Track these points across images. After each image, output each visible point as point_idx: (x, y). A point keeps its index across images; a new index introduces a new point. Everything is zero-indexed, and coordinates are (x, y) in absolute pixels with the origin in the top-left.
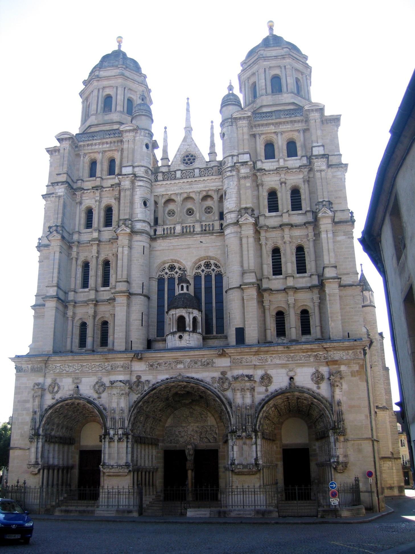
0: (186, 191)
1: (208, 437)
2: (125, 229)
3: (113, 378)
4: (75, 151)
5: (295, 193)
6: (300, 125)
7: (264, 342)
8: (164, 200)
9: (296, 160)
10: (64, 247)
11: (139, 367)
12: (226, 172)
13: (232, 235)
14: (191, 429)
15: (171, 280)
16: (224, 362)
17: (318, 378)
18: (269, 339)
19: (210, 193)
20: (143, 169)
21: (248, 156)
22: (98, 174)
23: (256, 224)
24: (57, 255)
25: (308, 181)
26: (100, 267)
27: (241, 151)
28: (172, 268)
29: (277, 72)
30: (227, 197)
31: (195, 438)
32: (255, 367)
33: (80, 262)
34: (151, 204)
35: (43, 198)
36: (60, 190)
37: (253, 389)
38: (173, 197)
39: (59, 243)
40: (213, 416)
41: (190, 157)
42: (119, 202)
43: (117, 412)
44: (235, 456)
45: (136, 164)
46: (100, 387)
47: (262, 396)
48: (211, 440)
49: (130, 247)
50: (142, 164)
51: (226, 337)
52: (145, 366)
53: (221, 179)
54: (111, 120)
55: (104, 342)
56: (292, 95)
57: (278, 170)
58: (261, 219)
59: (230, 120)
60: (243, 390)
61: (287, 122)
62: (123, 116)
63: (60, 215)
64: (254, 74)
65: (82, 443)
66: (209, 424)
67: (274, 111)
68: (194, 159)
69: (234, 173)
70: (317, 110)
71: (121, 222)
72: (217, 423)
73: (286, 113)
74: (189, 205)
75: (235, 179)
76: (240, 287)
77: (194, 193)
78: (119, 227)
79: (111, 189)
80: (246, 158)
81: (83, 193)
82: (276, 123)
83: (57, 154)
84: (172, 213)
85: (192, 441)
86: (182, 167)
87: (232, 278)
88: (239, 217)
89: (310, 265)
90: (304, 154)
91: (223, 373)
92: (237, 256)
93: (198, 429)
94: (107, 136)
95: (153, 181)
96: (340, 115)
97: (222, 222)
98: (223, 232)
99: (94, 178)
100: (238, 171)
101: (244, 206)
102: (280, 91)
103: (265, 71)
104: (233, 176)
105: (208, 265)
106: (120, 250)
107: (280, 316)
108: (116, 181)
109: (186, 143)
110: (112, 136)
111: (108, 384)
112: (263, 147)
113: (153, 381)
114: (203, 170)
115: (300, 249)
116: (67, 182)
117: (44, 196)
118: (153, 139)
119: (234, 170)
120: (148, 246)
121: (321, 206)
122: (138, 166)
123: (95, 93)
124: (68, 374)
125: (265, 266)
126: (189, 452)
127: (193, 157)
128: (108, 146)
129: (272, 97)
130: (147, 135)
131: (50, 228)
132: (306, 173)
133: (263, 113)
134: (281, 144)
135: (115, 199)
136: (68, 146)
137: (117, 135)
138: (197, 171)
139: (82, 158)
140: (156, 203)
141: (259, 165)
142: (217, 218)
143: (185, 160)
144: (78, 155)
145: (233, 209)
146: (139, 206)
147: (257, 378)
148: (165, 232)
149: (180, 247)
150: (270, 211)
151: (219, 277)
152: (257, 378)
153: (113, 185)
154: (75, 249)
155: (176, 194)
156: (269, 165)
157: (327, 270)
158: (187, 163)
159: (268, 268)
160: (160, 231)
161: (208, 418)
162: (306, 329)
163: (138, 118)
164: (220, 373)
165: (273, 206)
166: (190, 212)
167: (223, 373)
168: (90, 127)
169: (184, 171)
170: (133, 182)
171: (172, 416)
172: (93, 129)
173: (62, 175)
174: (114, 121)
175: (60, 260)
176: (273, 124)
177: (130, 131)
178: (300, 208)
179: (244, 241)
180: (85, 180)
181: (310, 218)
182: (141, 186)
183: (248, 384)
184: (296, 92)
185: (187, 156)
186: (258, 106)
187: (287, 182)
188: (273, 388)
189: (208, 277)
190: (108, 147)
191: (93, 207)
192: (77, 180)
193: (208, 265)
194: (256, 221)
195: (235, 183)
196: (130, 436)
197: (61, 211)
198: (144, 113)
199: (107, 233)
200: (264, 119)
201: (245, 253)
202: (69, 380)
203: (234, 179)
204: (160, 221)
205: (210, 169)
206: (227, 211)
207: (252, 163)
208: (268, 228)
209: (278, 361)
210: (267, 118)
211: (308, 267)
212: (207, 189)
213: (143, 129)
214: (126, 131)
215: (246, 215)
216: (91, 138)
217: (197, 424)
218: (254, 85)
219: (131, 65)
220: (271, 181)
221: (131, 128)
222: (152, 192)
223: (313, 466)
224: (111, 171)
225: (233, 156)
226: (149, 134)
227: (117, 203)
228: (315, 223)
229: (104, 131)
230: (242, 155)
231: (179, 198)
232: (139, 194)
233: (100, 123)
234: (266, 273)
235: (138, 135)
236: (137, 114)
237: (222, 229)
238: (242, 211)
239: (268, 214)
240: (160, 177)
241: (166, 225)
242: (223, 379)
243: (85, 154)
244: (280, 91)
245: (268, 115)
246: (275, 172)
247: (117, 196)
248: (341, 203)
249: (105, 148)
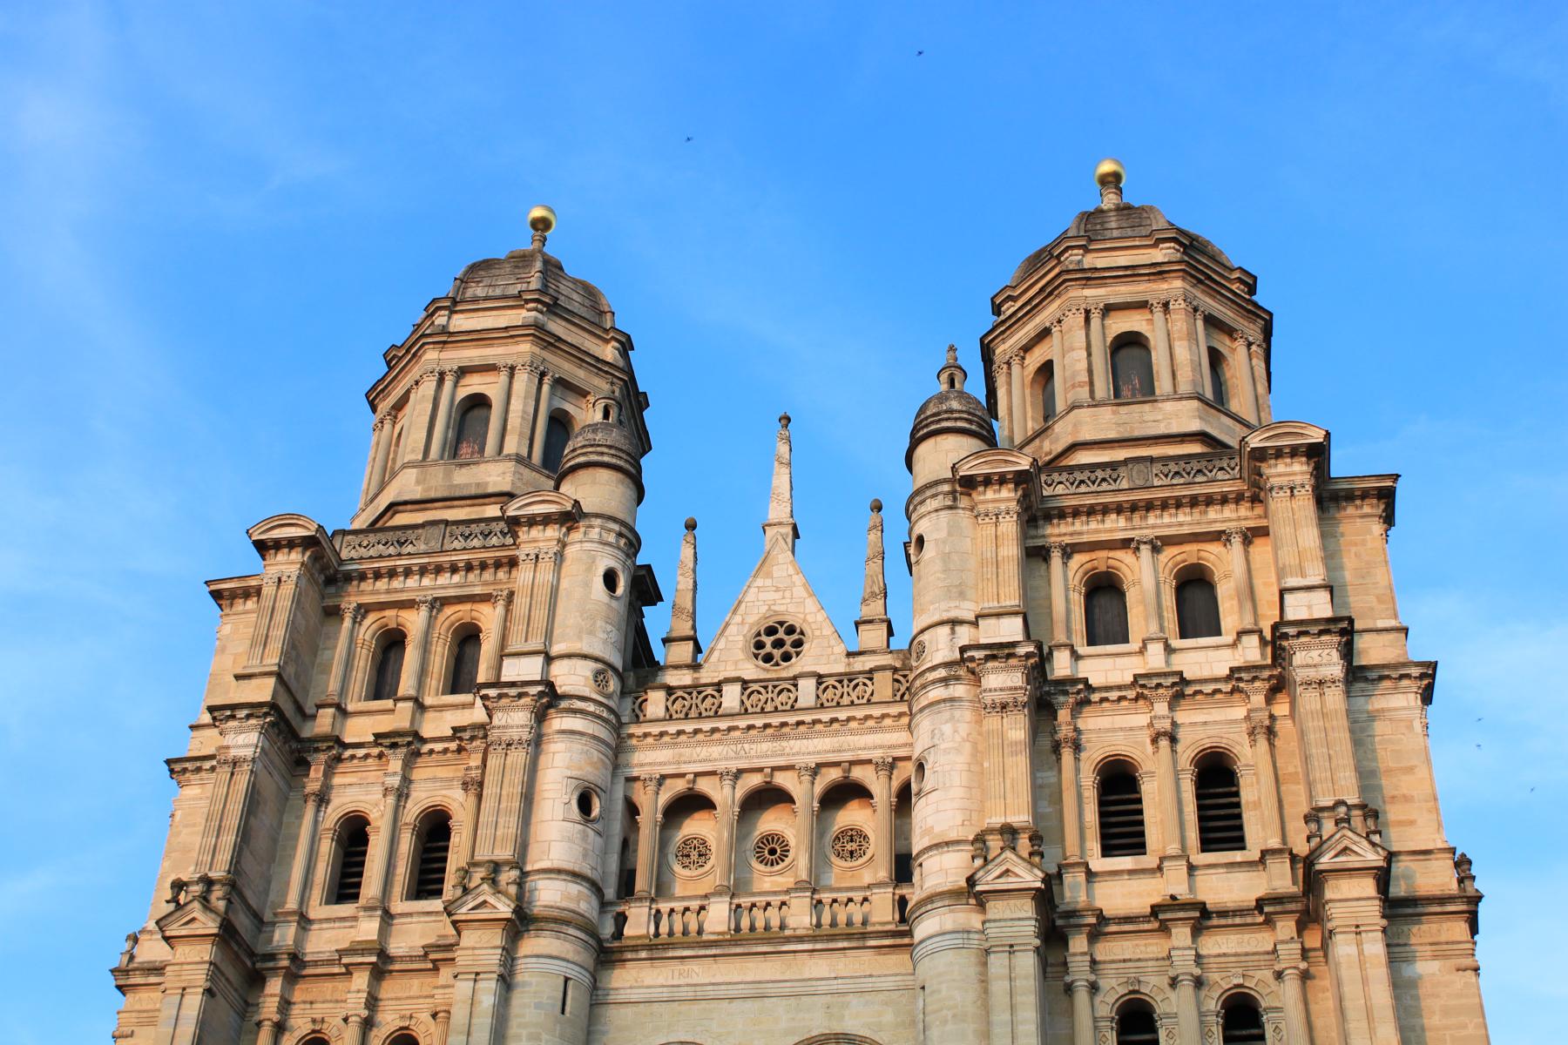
0: (757, 763)
2: (491, 900)
4: (323, 597)
5: (1215, 775)
6: (1228, 512)
8: (664, 797)
9: (1217, 647)
10: (230, 972)
12: (924, 686)
13: (947, 941)
19: (858, 773)
21: (1018, 622)
22: (407, 685)
23: (1046, 898)
24: (194, 1002)
25: (1270, 732)
27: (991, 605)
30: (928, 783)
35: (172, 771)
36: (241, 739)
38: (704, 786)
39: (205, 952)
41: (781, 634)
42: (480, 797)
49: (506, 981)
50: (586, 650)
53: (905, 720)
54: (478, 485)
56: (1195, 403)
57: (1141, 688)
58: (1074, 884)
59: (946, 488)
61: (1178, 504)
62: (526, 472)
63: (229, 839)
64: (1045, 333)
67: (1126, 462)
68: (798, 644)
69: (959, 690)
70: (1294, 452)
71: (478, 874)
73: (1173, 467)
77: (789, 774)
78: (466, 891)
79: (453, 746)
80: (1010, 629)
81: (339, 759)
82: (1134, 507)
83: (251, 604)
84: (696, 852)
86: (751, 670)
88: (979, 862)
90: (1248, 623)
94: (456, 544)
95: (625, 719)
96: (1396, 477)
97: (904, 890)
98: (909, 934)
99: (389, 703)
102: (1147, 392)
103: (1087, 320)
104: (952, 700)
108: (478, 714)
109: (768, 582)
110: (476, 543)
112: (1078, 600)
114: (831, 681)
116: (273, 706)
117: (177, 767)
118: (640, 560)
119: (958, 678)
120: (586, 979)
121: (1328, 827)
122: (569, 656)
123: (429, 387)
127: (795, 637)
128: (456, 578)
129: (1114, 413)
130: (612, 538)
131: (179, 886)
132: (1258, 700)
133: (1082, 468)
134: (1146, 582)
135: (465, 786)
136: (294, 570)
137: (494, 541)
138: (807, 687)
139: (347, 623)
141: (1061, 665)
142: (883, 872)
143: (760, 645)
144: (334, 613)
145: (953, 836)
146: (559, 812)
148: (664, 929)
149: (722, 991)
153: (463, 729)
158: (768, 658)
160: (638, 922)
163: (583, 475)
165: (1122, 829)
166: (773, 851)
168: (393, 507)
169: (755, 687)
170: (541, 716)
172: (401, 519)
173: (254, 682)
174: (490, 490)
175: (203, 1024)
176: (1119, 509)
177: (546, 520)
178: (1238, 843)
179: (998, 962)
180: (350, 707)
182: (573, 732)
184: (1209, 394)
185: (771, 631)
186: (1059, 448)
187: (1182, 734)
190: (457, 586)
191: (373, 816)
192: (319, 707)
194: (1047, 879)
195: (964, 729)
197: (233, 820)
198: (606, 459)
199: (418, 926)
200: (1083, 489)
201: (1001, 1017)
203: (957, 713)
204: (641, 883)
205: (861, 679)
206: (926, 842)
207: (1031, 649)
208: (1101, 927)
210: (1094, 488)
212: (848, 756)
213: (597, 516)
214: (532, 521)
215: (1008, 854)
216: (392, 550)
218: (1046, 370)
219: (575, 296)
220: (1111, 731)
221: (552, 508)
222: (616, 767)
224: (460, 678)
225: (954, 623)
226: (620, 535)
227: (472, 799)
228: (1308, 901)
229: (447, 523)
230: (992, 621)
231: (727, 790)
233: (433, 495)
235: (576, 536)
236: (582, 459)
237: (903, 920)
239: (1098, 863)
241: (673, 898)
243: (363, 610)
244: (1147, 392)
245: (1100, 474)
246: (1131, 694)
247: (475, 774)
248: (1412, 823)
249: (443, 587)
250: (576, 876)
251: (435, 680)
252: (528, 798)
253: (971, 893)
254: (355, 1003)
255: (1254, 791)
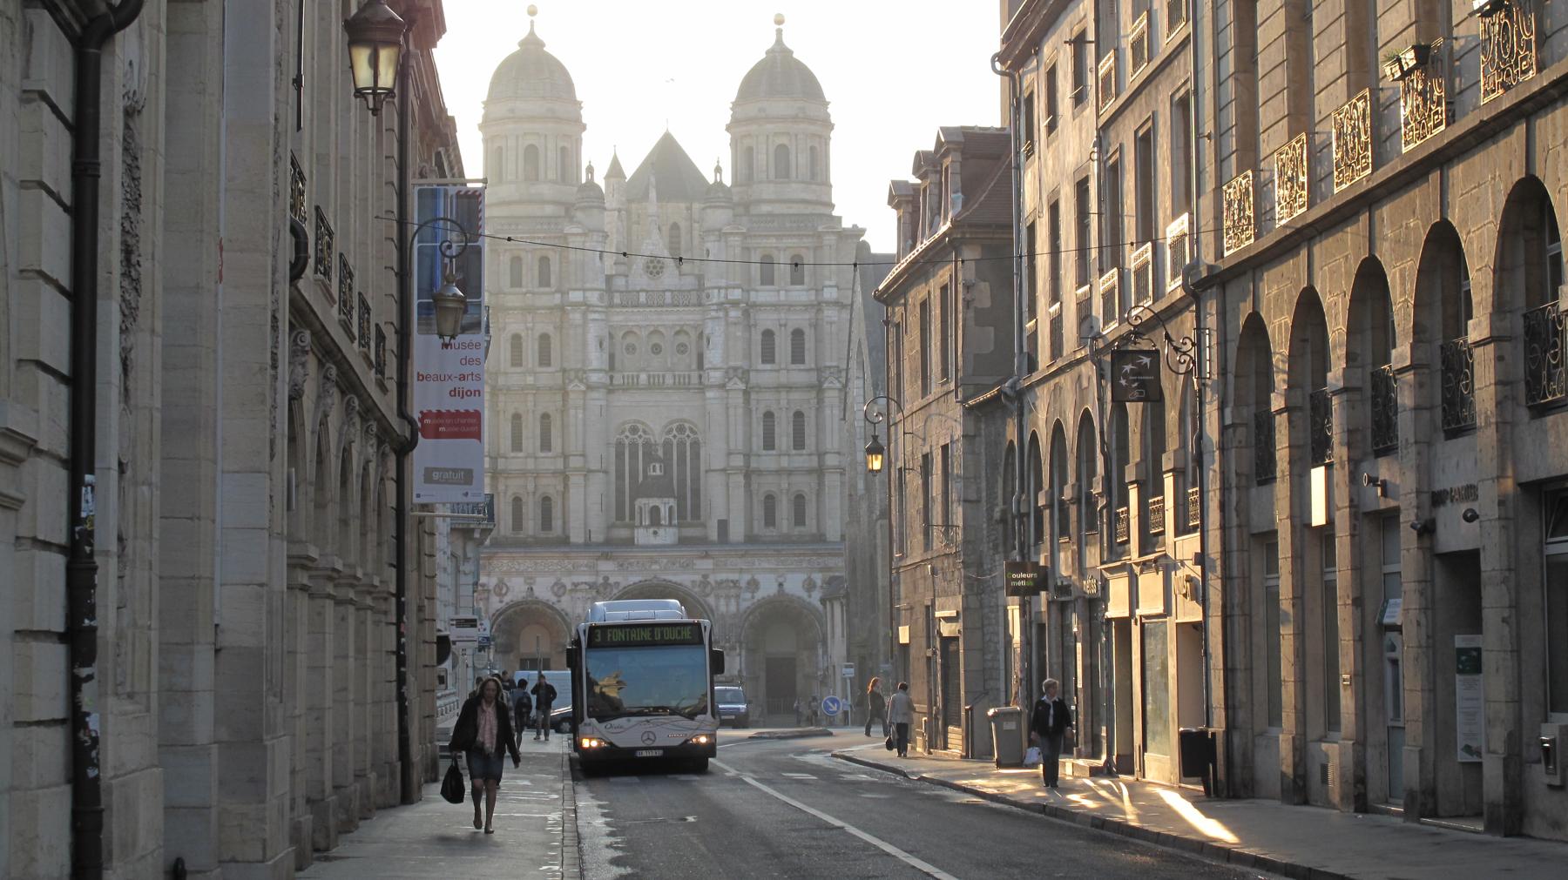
3: (576, 579)
7: (751, 539)
11: (606, 567)
15: (634, 445)
16: (707, 564)
17: (810, 586)
18: (756, 531)
20: (596, 294)
26: (538, 424)
28: (634, 430)
29: (784, 140)
32: (741, 571)
33: (509, 416)
34: (606, 344)
37: (738, 596)
45: (588, 286)
46: (559, 588)
47: (747, 604)
51: (704, 526)
55: (547, 523)
60: (728, 597)
65: (522, 650)
69: (721, 314)
74: (656, 340)
75: (723, 323)
76: (724, 470)
80: (736, 294)
84: (631, 349)
87: (713, 455)
89: (810, 441)
91: (705, 577)
92: (722, 433)
100: (727, 315)
101: (732, 364)
105: (681, 429)
106: (572, 412)
107: (770, 501)
111: (569, 587)
113: (623, 584)
115: (799, 415)
124: (519, 573)
125: (754, 439)
138: (668, 294)
140: (611, 336)
142: (694, 366)
147: (743, 584)
150: (764, 362)
151: (696, 445)
152: (743, 584)
154: (502, 398)
155: (639, 327)
156: (764, 295)
157: (828, 457)
159: (758, 442)
160: (618, 380)
162: (800, 519)
165: (768, 356)
167: (705, 577)
170: (584, 314)
178: (803, 362)
179: (731, 411)
181: (812, 378)
183: (733, 592)
188: (760, 595)
189: (681, 444)
193: (681, 429)
202: (520, 580)
204: (618, 365)
209: (766, 565)
211: (807, 442)
223: (799, 676)
225: (719, 288)
232: (593, 332)
234: (755, 448)
238: (731, 372)
239: (761, 366)
240: (617, 300)
242: (705, 583)
250: (600, 370)
251: (536, 282)
252: (584, 344)
253: (722, 386)
254: (530, 404)
255: (809, 344)
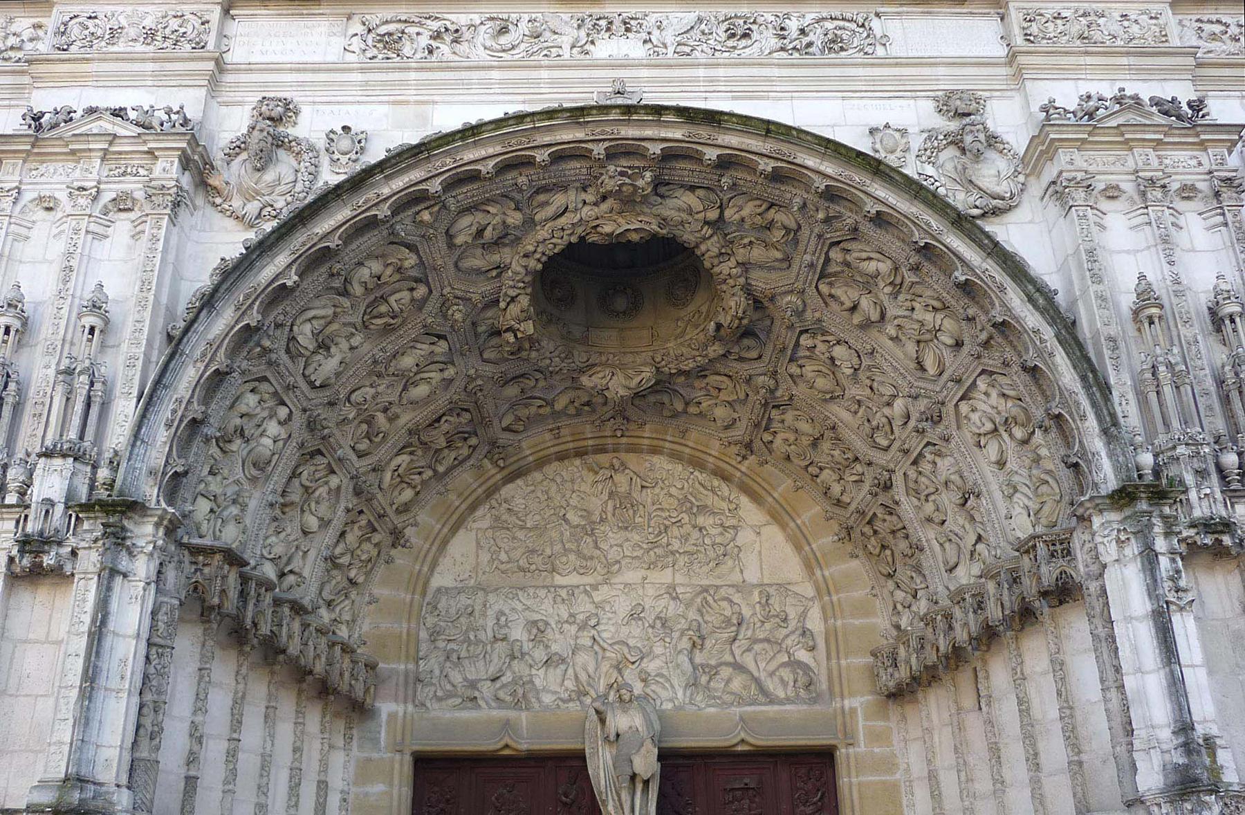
1: (748, 661)
14: (623, 606)
31: (652, 666)
40: (779, 516)
43: (47, 331)
44: (1203, 709)
48: (772, 685)
52: (339, 42)
66: (752, 576)
72: (810, 564)
85: (638, 688)
93: (673, 609)
126: (623, 760)
161: (745, 537)
164: (930, 105)
171: (482, 519)
196: (145, 533)
217: (666, 577)
